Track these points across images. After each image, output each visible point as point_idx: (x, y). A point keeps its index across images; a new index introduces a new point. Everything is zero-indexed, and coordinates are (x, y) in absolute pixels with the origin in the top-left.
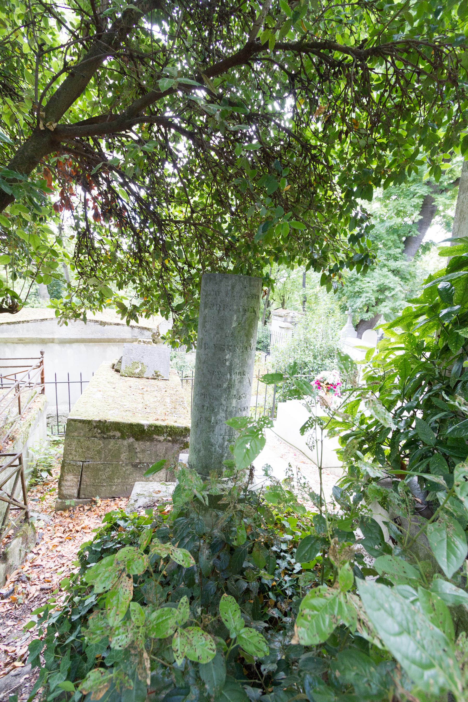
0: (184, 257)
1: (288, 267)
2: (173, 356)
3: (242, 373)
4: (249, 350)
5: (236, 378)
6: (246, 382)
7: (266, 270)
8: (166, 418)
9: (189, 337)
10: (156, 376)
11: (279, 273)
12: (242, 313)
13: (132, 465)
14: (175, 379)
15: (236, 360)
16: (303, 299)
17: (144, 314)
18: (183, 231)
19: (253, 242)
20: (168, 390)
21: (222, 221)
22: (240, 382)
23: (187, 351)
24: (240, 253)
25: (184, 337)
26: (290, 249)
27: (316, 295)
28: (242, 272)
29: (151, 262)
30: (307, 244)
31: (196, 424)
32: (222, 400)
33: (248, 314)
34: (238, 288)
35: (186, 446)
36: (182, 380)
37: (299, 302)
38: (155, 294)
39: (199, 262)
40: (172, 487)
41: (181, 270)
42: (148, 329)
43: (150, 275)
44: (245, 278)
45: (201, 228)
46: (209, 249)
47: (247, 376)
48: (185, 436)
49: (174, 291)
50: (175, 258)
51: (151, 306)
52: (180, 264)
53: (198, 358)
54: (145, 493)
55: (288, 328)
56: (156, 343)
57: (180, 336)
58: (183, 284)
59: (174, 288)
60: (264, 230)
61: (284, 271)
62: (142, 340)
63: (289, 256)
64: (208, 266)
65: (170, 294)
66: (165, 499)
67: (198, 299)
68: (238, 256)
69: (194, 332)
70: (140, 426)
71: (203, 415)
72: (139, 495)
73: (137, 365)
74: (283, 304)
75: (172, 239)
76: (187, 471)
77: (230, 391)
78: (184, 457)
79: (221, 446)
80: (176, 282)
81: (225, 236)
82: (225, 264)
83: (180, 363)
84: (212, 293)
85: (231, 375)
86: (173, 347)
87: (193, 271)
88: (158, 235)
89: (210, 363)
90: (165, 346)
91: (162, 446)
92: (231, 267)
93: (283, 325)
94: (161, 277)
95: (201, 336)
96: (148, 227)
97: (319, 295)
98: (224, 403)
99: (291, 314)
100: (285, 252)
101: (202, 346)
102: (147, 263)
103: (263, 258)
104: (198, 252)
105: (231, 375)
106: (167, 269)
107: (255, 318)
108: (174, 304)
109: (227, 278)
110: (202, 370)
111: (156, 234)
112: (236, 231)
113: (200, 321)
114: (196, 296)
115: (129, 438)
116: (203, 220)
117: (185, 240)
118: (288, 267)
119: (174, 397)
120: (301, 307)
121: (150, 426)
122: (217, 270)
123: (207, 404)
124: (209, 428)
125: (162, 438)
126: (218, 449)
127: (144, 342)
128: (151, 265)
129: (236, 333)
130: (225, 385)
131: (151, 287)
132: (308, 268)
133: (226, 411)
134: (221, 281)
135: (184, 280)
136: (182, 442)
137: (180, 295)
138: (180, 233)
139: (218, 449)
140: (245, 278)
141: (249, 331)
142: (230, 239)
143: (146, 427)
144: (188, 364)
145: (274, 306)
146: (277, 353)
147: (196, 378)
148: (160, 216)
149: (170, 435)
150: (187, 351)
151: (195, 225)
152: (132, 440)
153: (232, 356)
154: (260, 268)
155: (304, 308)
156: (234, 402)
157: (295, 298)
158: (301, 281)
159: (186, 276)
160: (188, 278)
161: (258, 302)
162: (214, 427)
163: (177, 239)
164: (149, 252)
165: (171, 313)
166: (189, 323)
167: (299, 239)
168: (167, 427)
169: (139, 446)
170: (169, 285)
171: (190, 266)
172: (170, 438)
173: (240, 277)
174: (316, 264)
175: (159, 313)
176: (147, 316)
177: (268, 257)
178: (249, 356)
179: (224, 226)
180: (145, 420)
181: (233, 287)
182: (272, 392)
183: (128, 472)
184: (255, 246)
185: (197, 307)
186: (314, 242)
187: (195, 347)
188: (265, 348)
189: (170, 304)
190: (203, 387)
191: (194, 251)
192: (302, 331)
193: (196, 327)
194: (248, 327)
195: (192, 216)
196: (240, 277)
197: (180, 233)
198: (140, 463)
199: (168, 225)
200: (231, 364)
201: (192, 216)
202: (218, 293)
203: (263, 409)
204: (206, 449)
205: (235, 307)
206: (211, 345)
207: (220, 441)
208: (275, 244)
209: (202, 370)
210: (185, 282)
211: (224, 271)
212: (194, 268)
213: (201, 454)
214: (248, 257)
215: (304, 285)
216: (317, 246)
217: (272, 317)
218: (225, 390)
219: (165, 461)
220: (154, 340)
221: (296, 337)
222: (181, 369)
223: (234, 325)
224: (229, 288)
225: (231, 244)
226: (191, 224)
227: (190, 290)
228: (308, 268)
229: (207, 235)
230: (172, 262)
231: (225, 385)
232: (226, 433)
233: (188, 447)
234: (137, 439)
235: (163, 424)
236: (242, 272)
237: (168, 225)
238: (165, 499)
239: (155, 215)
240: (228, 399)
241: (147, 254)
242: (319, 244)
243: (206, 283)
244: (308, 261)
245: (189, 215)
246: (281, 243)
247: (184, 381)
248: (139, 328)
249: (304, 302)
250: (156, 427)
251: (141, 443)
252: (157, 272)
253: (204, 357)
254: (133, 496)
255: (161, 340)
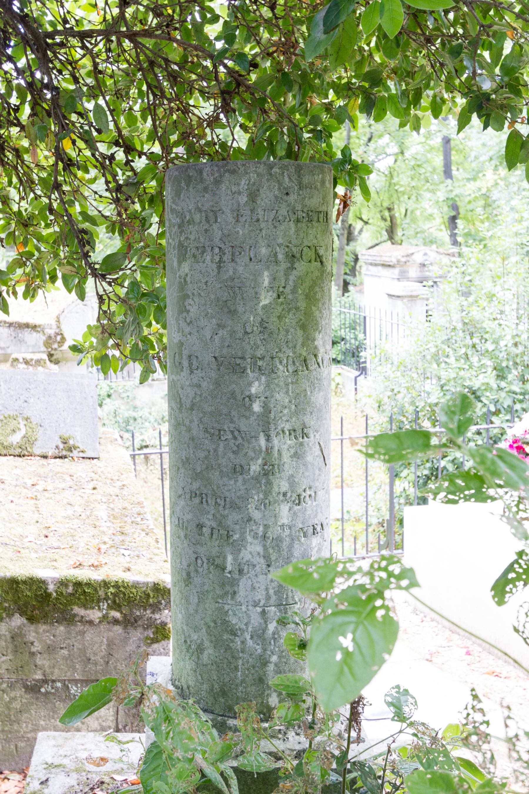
0: (111, 125)
1: (402, 125)
2: (104, 393)
3: (301, 432)
4: (313, 367)
5: (283, 445)
6: (312, 455)
7: (338, 140)
8: (102, 559)
9: (145, 340)
10: (66, 451)
11: (375, 142)
12: (284, 266)
13: (26, 687)
14: (116, 455)
15: (281, 397)
16: (449, 213)
17: (21, 289)
18: (104, 56)
19: (297, 66)
20: (99, 485)
21: (203, 17)
22: (296, 456)
23: (143, 379)
24: (263, 100)
25: (131, 341)
26: (405, 73)
27: (486, 197)
28: (273, 152)
29: (27, 151)
30: (456, 52)
31: (187, 575)
32: (251, 508)
33: (301, 267)
34: (266, 196)
35: (161, 633)
36: (133, 457)
37: (438, 221)
38: (45, 232)
39: (153, 136)
40: (135, 746)
41: (105, 164)
42: (34, 327)
43: (27, 183)
44: (283, 168)
45: (149, 43)
46: (178, 98)
47: (312, 440)
48: (156, 608)
49: (93, 221)
50: (89, 133)
51: (38, 267)
52: (102, 148)
53: (175, 396)
54: (66, 762)
55: (413, 298)
56: (57, 362)
57: (120, 337)
58: (116, 201)
59: (92, 212)
60: (330, 26)
61: (386, 139)
62: (20, 356)
63: (405, 93)
64: (177, 144)
65: (84, 231)
66: (119, 778)
67: (160, 236)
68: (258, 106)
69: (156, 326)
70: (36, 584)
71: (202, 550)
72: (50, 766)
73: (13, 424)
74: (391, 232)
75: (76, 80)
76: (173, 705)
77: (269, 483)
78: (161, 666)
79: (260, 635)
80: (95, 196)
81: (217, 58)
82: (222, 133)
83: (125, 412)
84: (197, 217)
85: (268, 439)
86: (105, 372)
87: (140, 163)
88: (38, 75)
89: (208, 408)
90: (83, 369)
91: (96, 635)
92: (241, 140)
93: (400, 288)
94: (57, 186)
95: (177, 337)
96: (10, 59)
97: (495, 195)
98: (256, 515)
99: (419, 258)
100: (391, 84)
101: (182, 362)
102: (17, 153)
103: (328, 107)
104: (149, 110)
105: (268, 439)
106: (69, 164)
107: (322, 276)
108: (100, 253)
109: (233, 172)
110: (189, 430)
111: (32, 75)
112: (247, 40)
113: (170, 298)
114: (154, 230)
115: (10, 616)
116: (152, 21)
117: (109, 82)
118: (402, 125)
119: (119, 504)
120: (445, 235)
121: (63, 583)
122: (203, 153)
123: (209, 522)
124: (223, 585)
125: (95, 615)
126: (250, 643)
127: (27, 362)
128: (26, 157)
129: (273, 323)
130: (255, 468)
131: (31, 217)
132: (463, 122)
133: (264, 537)
134: (217, 182)
135: (119, 188)
136: (150, 624)
137: (111, 229)
138: (95, 65)
139: (250, 643)
140: (283, 168)
141: (308, 314)
142: (230, 63)
143: (51, 588)
144: (145, 413)
145: (365, 238)
146: (387, 369)
147: (174, 452)
148: (41, 26)
149: (116, 606)
150: (143, 379)
151: (132, 36)
152: (18, 620)
153: (268, 385)
154: (323, 135)
155: (453, 236)
156: (284, 512)
157: (428, 211)
158: (438, 161)
159: (121, 179)
160: (127, 183)
161: (327, 231)
162: (234, 583)
163: (90, 81)
164: (19, 124)
165: (91, 281)
166: (141, 303)
167: (429, 40)
168: (106, 584)
169: (38, 635)
170: (78, 208)
171: (129, 149)
172: (117, 615)
173: (271, 167)
174: (485, 107)
175: (59, 282)
176: (30, 293)
177: (341, 103)
178: (316, 384)
179: (212, 31)
180: (50, 569)
181: (253, 196)
182: (386, 478)
183: (16, 705)
184: (304, 75)
185: (158, 258)
186: (475, 44)
187: (164, 367)
188: (353, 356)
189: (86, 256)
190: (196, 476)
191: (137, 108)
192: (455, 302)
193: (160, 311)
194: (304, 304)
195: (122, 14)
196: (271, 167)
197: (95, 65)
198: (45, 681)
199: (62, 45)
200: (267, 409)
201: (122, 14)
202: (212, 215)
203: (362, 526)
204: (217, 643)
205: (264, 251)
206: (208, 358)
207: (256, 620)
208: (360, 64)
209: (189, 430)
210: (120, 194)
211: (223, 154)
212: (140, 155)
213: (205, 657)
214: (286, 109)
215: (448, 173)
216: (486, 55)
217: (362, 267)
218: (256, 479)
219: (114, 682)
220: (50, 355)
221: (438, 319)
222: (127, 425)
223: (266, 299)
224: (243, 199)
225: (237, 80)
226: (120, 35)
227: (135, 216)
228: (463, 122)
229: (167, 61)
230: (81, 144)
231: (255, 468)
232: (268, 597)
233: (166, 637)
234: (31, 619)
235: (96, 576)
236: (273, 152)
237: (62, 45)
238: (119, 778)
239: (26, 25)
240: (266, 504)
241: (14, 130)
242: (490, 47)
243: (178, 194)
244: (461, 101)
245: (116, 11)
246: (377, 58)
247: (140, 459)
248: (11, 325)
249: (453, 219)
250: (78, 584)
251: (42, 627)
252: (44, 175)
253: (190, 392)
254: (36, 769)
255: (71, 353)
